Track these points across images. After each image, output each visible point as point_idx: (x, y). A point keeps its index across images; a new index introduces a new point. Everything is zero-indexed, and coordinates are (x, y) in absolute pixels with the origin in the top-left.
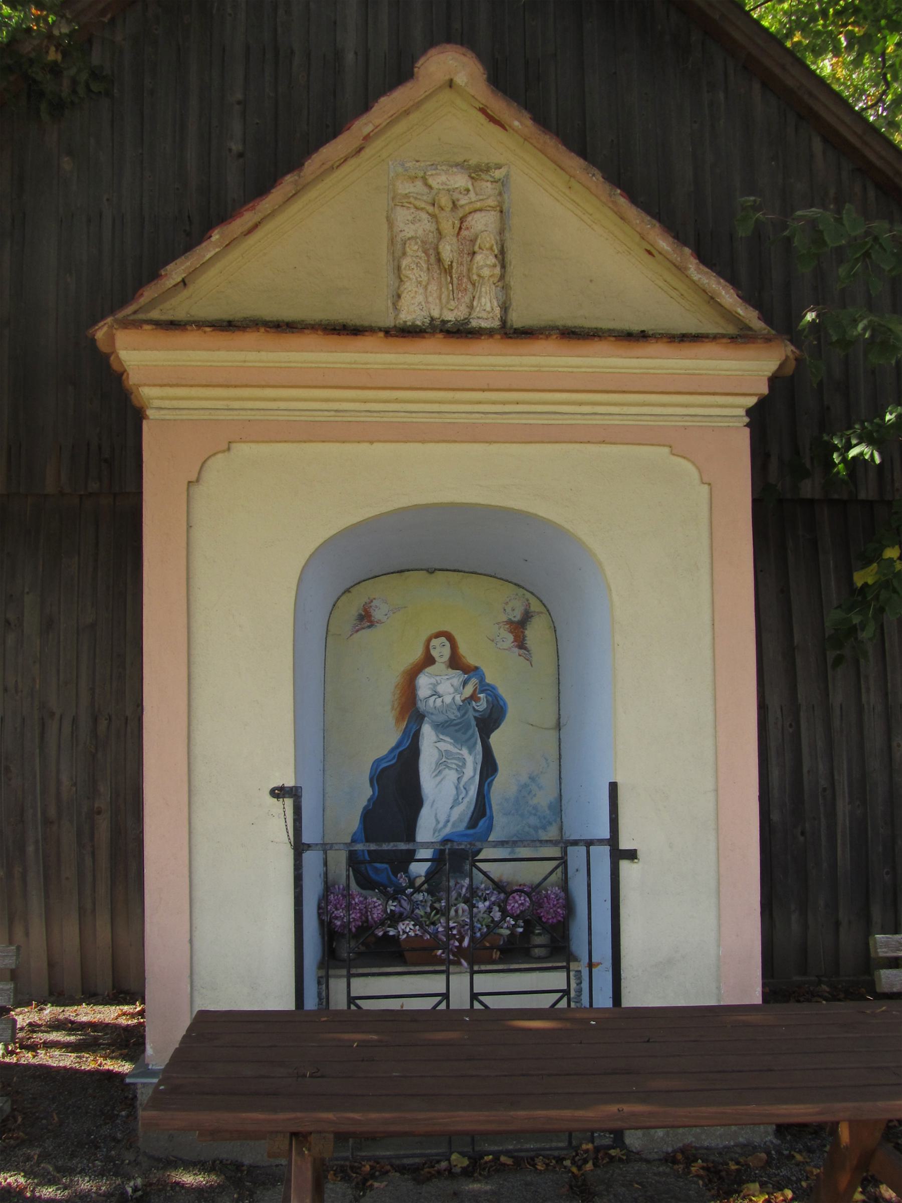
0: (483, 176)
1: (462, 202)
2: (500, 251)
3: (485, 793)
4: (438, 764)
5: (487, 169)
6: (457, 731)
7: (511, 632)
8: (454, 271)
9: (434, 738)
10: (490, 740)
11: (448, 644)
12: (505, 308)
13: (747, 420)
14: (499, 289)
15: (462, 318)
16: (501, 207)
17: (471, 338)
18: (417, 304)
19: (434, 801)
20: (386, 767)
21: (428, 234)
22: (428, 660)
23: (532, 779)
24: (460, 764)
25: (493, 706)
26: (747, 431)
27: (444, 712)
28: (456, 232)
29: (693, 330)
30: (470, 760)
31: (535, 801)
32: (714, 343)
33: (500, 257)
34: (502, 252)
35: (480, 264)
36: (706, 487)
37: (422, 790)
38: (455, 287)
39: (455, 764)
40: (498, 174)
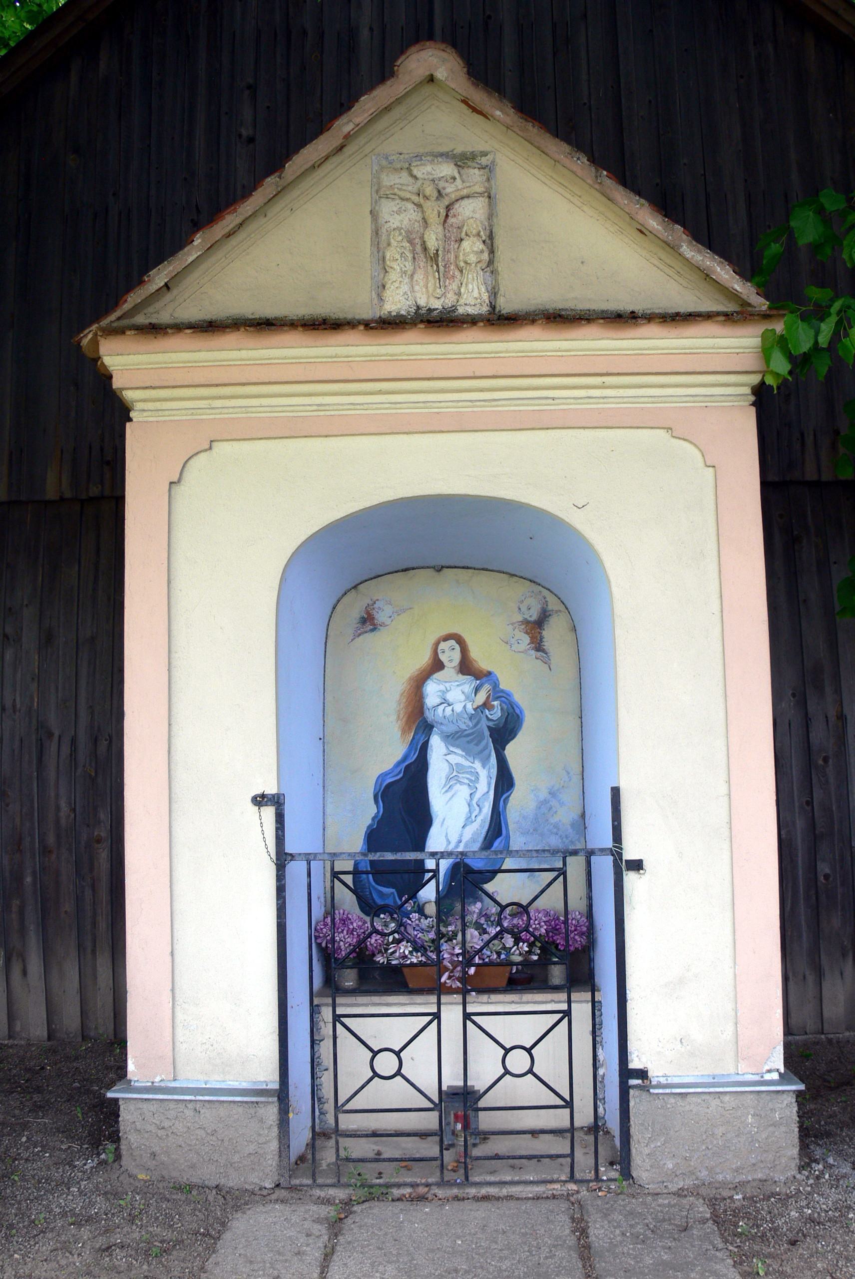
0: (470, 163)
1: (448, 190)
2: (489, 236)
3: (501, 810)
4: (449, 779)
5: (473, 157)
6: (468, 742)
7: (527, 633)
8: (440, 259)
9: (444, 751)
10: (505, 752)
11: (457, 647)
12: (494, 293)
13: (753, 398)
14: (488, 274)
15: (450, 305)
16: (490, 193)
17: (452, 327)
19: (444, 820)
20: (392, 782)
22: (437, 665)
23: (553, 794)
24: (473, 779)
25: (508, 714)
26: (753, 409)
27: (455, 721)
28: (442, 220)
29: (683, 309)
30: (483, 774)
31: (554, 820)
32: (710, 321)
33: (488, 241)
34: (491, 236)
35: (467, 251)
36: (711, 469)
37: (431, 808)
38: (441, 275)
39: (467, 779)
40: (484, 161)
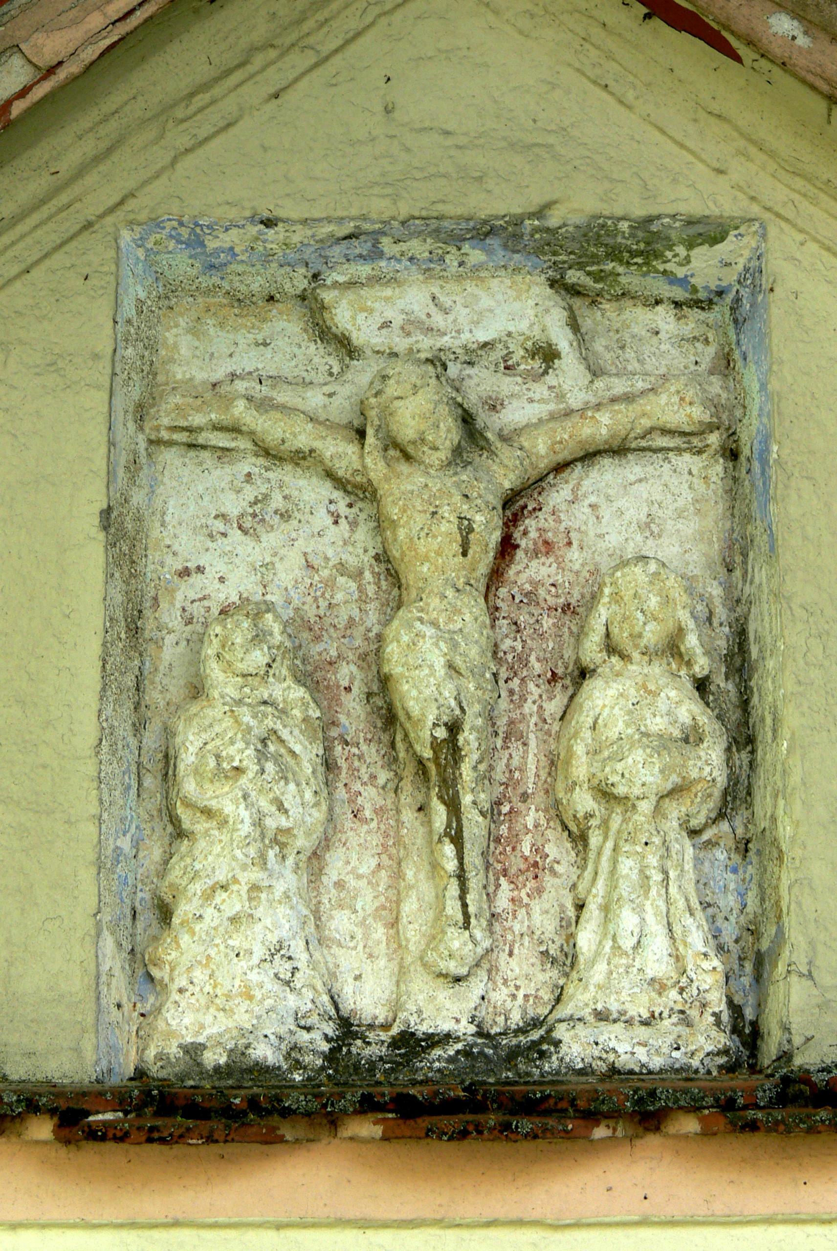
8: (466, 770)
15: (516, 1019)
18: (259, 952)
21: (329, 584)
28: (483, 569)
35: (612, 733)
38: (473, 858)
